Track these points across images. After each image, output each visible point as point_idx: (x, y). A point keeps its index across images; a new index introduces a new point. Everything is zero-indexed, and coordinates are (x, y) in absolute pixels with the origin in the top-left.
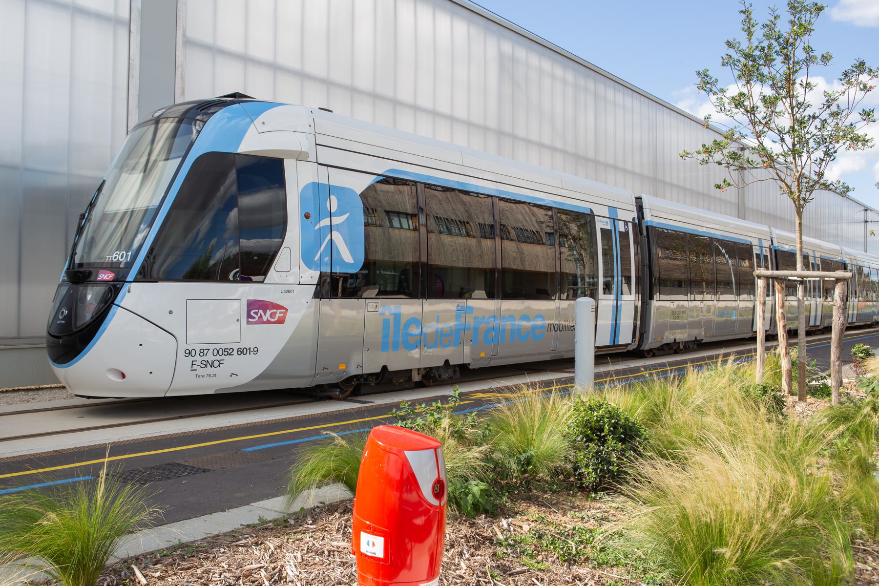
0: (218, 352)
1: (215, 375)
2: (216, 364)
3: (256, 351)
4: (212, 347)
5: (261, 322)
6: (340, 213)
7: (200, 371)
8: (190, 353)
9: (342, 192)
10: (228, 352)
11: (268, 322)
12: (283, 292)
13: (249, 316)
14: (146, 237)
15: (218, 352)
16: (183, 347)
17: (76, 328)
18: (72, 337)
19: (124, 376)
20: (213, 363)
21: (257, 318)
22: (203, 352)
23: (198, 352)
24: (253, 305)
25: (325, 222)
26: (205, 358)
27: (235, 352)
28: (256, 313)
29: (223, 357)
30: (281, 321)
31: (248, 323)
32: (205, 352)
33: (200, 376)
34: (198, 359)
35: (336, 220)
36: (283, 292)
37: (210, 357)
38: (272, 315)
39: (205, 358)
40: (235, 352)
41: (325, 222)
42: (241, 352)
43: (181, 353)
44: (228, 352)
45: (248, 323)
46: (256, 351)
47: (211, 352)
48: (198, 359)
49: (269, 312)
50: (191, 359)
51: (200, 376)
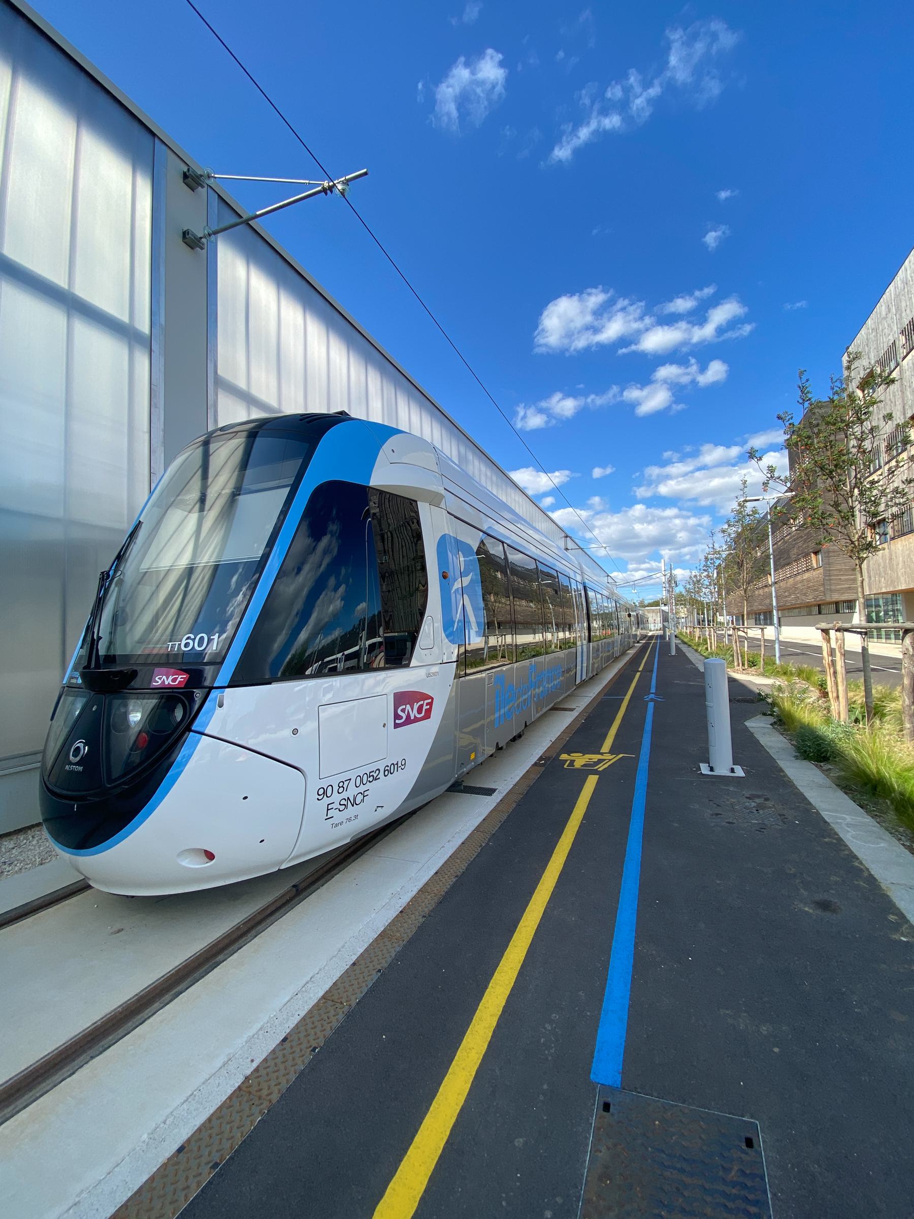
0: (362, 780)
1: (356, 817)
2: (360, 797)
4: (352, 775)
5: (409, 721)
7: (337, 816)
8: (325, 793)
11: (417, 720)
13: (397, 716)
14: (245, 611)
15: (362, 780)
16: (315, 785)
17: (110, 781)
18: (101, 790)
20: (355, 800)
21: (404, 716)
22: (342, 787)
23: (336, 788)
26: (345, 795)
27: (381, 775)
28: (403, 711)
31: (396, 726)
32: (345, 786)
33: (337, 825)
37: (351, 792)
38: (420, 710)
39: (345, 795)
40: (381, 775)
42: (388, 771)
43: (312, 795)
45: (396, 726)
47: (353, 781)
48: (336, 798)
50: (326, 801)
51: (337, 825)
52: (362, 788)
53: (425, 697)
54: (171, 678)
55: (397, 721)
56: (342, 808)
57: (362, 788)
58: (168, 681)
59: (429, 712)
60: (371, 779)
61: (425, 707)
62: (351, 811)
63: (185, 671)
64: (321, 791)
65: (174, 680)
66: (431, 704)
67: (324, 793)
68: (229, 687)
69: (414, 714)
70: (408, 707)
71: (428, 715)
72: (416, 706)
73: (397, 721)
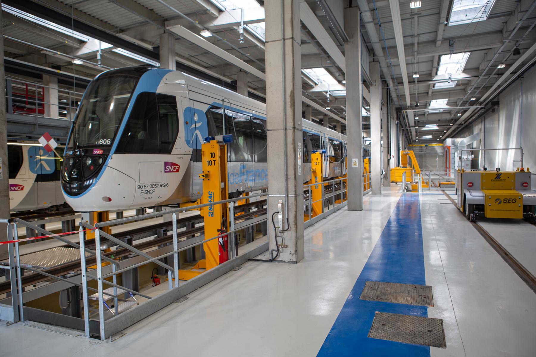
2: (151, 192)
3: (167, 185)
4: (149, 184)
5: (170, 171)
6: (198, 122)
9: (199, 112)
10: (156, 186)
11: (173, 172)
12: (179, 158)
13: (165, 169)
16: (138, 184)
19: (110, 200)
22: (146, 186)
24: (166, 164)
25: (194, 126)
26: (146, 189)
29: (154, 188)
30: (178, 171)
31: (165, 172)
34: (144, 189)
35: (198, 125)
36: (179, 158)
37: (149, 189)
38: (174, 168)
39: (146, 189)
41: (194, 126)
43: (137, 187)
44: (156, 186)
45: (165, 172)
46: (167, 185)
49: (173, 167)
50: (140, 189)
52: (152, 189)
53: (176, 165)
57: (152, 189)
62: (149, 195)
66: (179, 168)
67: (140, 187)
70: (170, 167)
71: (178, 171)
72: (173, 167)
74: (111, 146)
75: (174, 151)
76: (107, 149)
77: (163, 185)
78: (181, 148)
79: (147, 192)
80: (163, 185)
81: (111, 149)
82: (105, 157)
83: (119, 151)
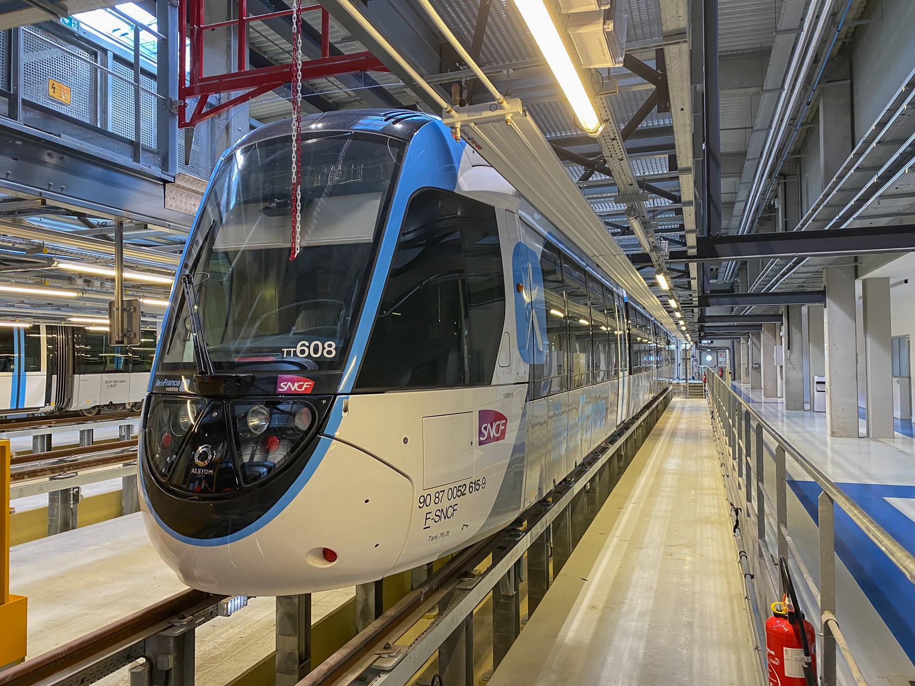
4: (446, 488)
5: (489, 440)
8: (425, 501)
10: (461, 492)
11: (498, 439)
13: (481, 434)
24: (490, 418)
26: (439, 506)
27: (467, 491)
28: (485, 428)
31: (481, 443)
37: (445, 504)
40: (467, 491)
45: (481, 443)
48: (433, 508)
50: (426, 509)
52: (453, 502)
54: (296, 385)
55: (482, 439)
56: (437, 519)
58: (295, 387)
59: (503, 432)
60: (459, 493)
61: (502, 428)
63: (311, 379)
64: (422, 500)
65: (300, 387)
66: (505, 425)
68: (351, 394)
69: (493, 432)
73: (482, 439)
74: (341, 361)
75: (499, 375)
76: (325, 373)
77: (476, 485)
78: (510, 365)
79: (443, 515)
80: (476, 485)
81: (339, 378)
82: (321, 405)
83: (368, 382)
